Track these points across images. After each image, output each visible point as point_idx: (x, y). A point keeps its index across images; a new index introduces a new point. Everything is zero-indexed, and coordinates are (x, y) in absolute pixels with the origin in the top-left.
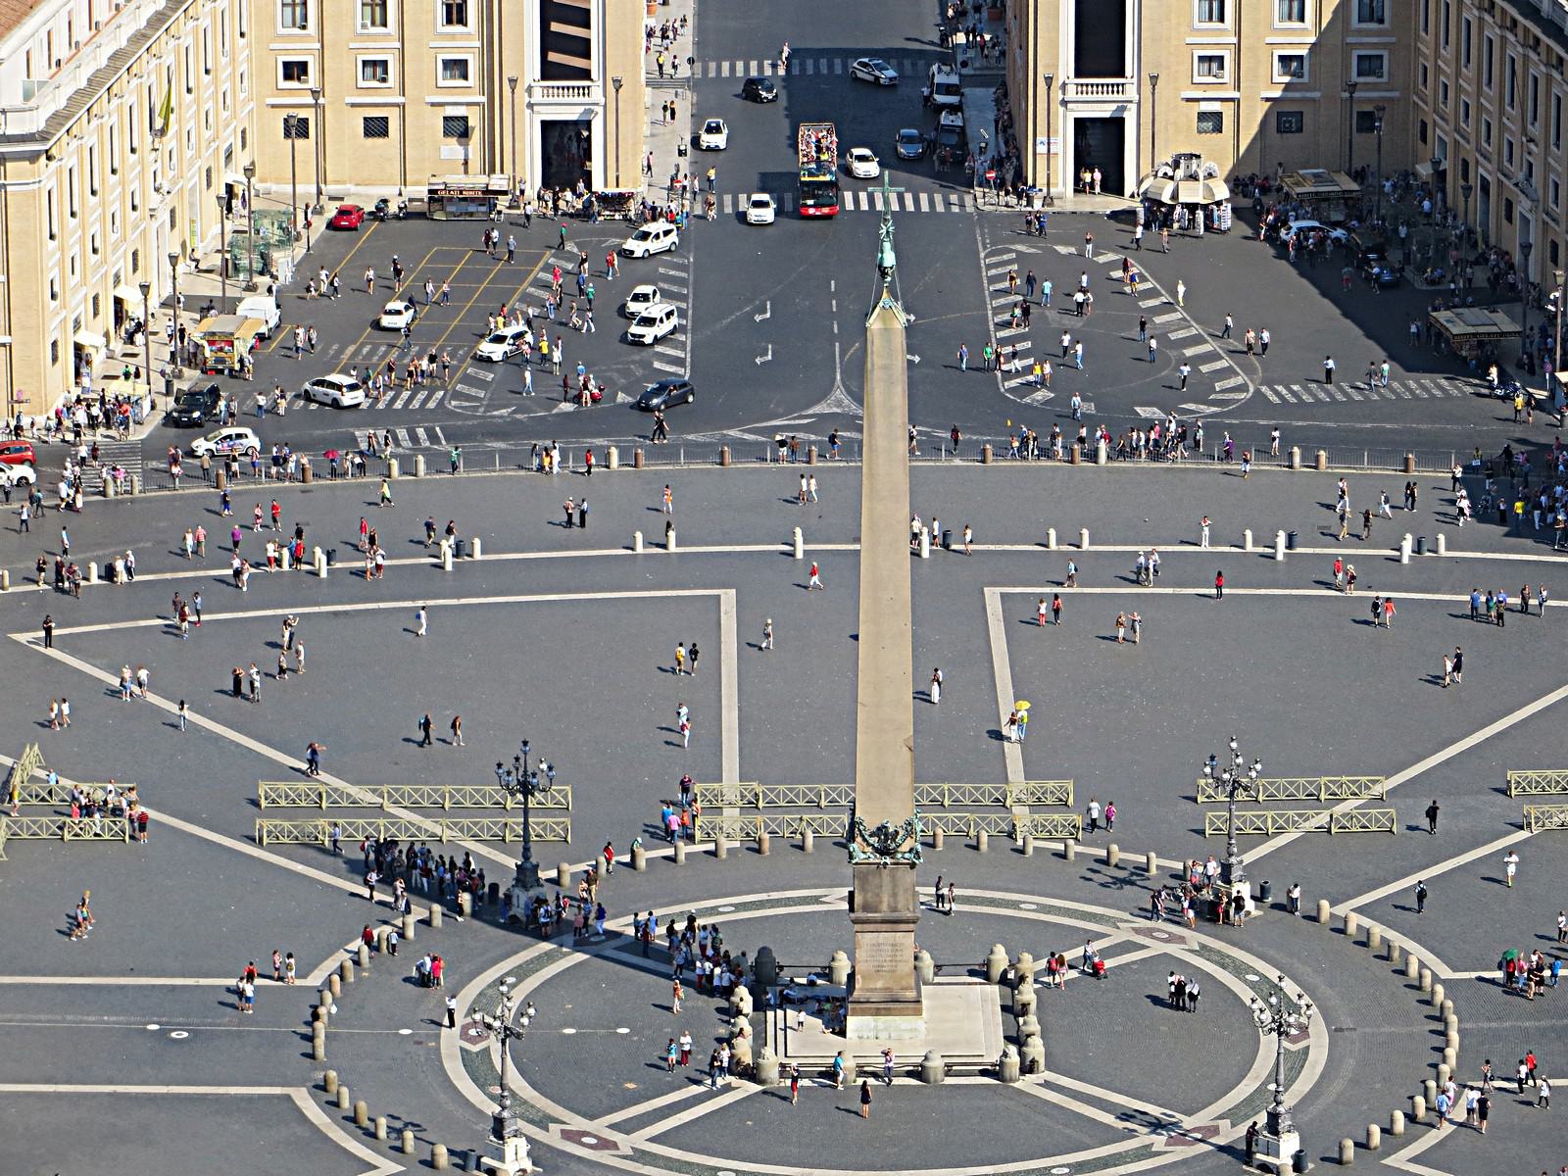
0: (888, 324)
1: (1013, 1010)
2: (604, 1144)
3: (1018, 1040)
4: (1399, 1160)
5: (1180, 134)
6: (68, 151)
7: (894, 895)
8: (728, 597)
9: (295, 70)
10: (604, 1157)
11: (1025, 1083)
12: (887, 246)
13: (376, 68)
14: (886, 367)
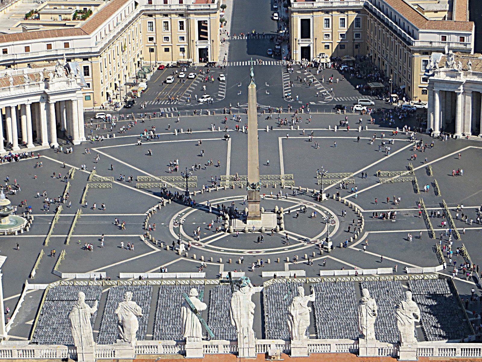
0: (252, 87)
1: (279, 219)
2: (199, 245)
3: (279, 224)
4: (351, 247)
5: (321, 49)
6: (104, 55)
7: (255, 197)
9: (151, 39)
10: (199, 248)
11: (281, 233)
12: (252, 72)
13: (166, 38)
14: (252, 95)
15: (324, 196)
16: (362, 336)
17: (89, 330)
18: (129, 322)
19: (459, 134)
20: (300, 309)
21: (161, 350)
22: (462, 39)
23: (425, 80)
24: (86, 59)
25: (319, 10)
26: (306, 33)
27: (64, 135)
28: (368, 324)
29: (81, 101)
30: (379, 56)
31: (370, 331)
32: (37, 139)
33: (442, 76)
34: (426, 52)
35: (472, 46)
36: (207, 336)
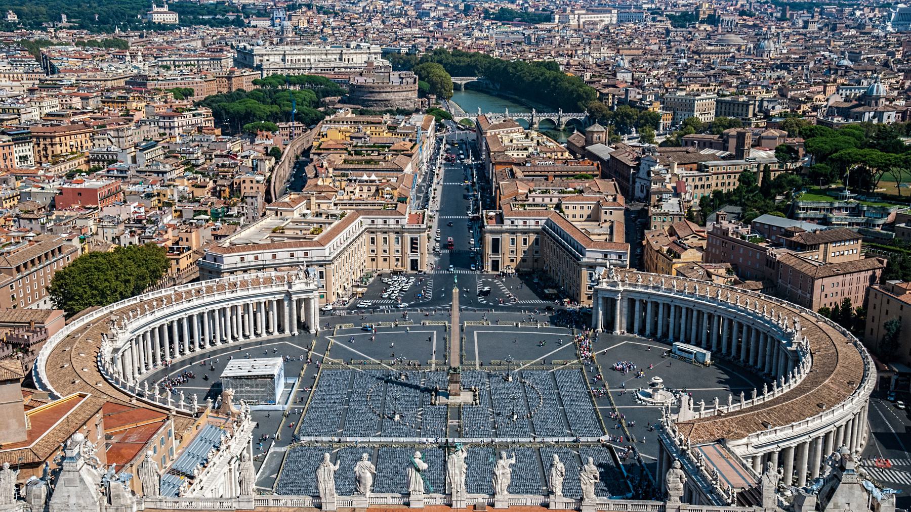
0: (456, 291)
1: (474, 396)
3: (475, 400)
5: (507, 263)
6: (336, 263)
8: (435, 332)
9: (373, 251)
13: (385, 251)
15: (510, 379)
16: (552, 493)
17: (331, 484)
18: (365, 478)
19: (618, 332)
20: (504, 468)
21: (391, 501)
22: (620, 257)
23: (590, 288)
24: (321, 266)
25: (507, 231)
26: (496, 249)
27: (304, 327)
28: (557, 482)
29: (317, 299)
30: (553, 268)
31: (558, 490)
32: (281, 329)
33: (604, 286)
34: (592, 267)
35: (628, 262)
36: (427, 491)
